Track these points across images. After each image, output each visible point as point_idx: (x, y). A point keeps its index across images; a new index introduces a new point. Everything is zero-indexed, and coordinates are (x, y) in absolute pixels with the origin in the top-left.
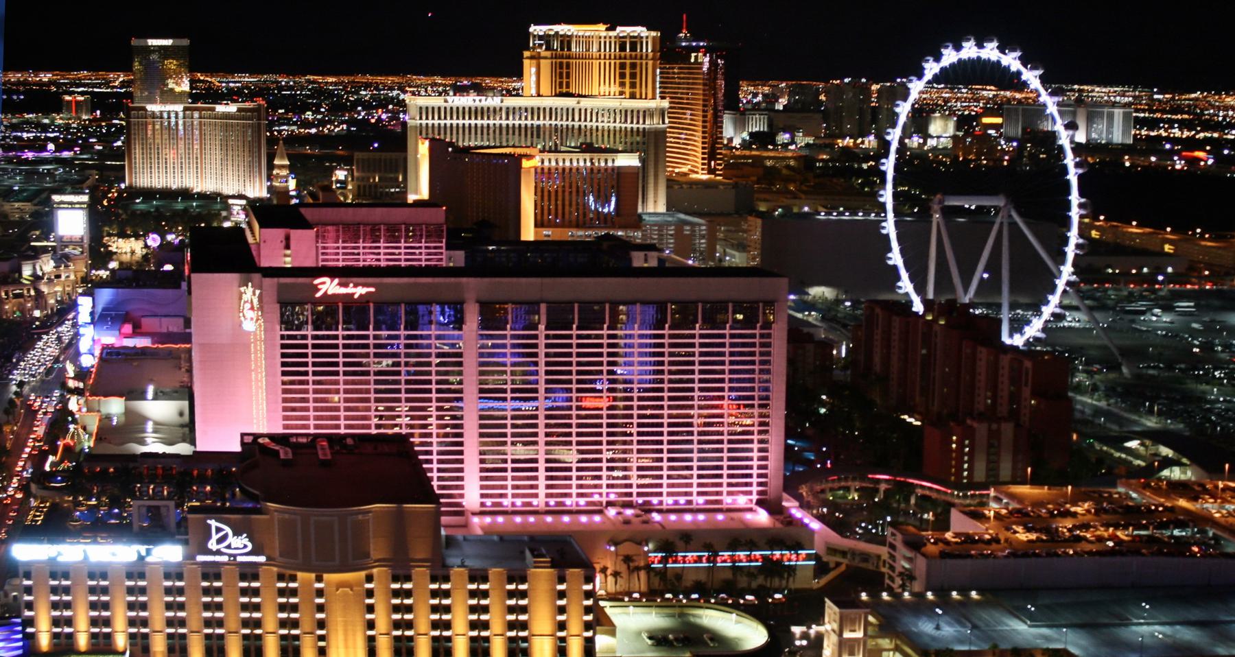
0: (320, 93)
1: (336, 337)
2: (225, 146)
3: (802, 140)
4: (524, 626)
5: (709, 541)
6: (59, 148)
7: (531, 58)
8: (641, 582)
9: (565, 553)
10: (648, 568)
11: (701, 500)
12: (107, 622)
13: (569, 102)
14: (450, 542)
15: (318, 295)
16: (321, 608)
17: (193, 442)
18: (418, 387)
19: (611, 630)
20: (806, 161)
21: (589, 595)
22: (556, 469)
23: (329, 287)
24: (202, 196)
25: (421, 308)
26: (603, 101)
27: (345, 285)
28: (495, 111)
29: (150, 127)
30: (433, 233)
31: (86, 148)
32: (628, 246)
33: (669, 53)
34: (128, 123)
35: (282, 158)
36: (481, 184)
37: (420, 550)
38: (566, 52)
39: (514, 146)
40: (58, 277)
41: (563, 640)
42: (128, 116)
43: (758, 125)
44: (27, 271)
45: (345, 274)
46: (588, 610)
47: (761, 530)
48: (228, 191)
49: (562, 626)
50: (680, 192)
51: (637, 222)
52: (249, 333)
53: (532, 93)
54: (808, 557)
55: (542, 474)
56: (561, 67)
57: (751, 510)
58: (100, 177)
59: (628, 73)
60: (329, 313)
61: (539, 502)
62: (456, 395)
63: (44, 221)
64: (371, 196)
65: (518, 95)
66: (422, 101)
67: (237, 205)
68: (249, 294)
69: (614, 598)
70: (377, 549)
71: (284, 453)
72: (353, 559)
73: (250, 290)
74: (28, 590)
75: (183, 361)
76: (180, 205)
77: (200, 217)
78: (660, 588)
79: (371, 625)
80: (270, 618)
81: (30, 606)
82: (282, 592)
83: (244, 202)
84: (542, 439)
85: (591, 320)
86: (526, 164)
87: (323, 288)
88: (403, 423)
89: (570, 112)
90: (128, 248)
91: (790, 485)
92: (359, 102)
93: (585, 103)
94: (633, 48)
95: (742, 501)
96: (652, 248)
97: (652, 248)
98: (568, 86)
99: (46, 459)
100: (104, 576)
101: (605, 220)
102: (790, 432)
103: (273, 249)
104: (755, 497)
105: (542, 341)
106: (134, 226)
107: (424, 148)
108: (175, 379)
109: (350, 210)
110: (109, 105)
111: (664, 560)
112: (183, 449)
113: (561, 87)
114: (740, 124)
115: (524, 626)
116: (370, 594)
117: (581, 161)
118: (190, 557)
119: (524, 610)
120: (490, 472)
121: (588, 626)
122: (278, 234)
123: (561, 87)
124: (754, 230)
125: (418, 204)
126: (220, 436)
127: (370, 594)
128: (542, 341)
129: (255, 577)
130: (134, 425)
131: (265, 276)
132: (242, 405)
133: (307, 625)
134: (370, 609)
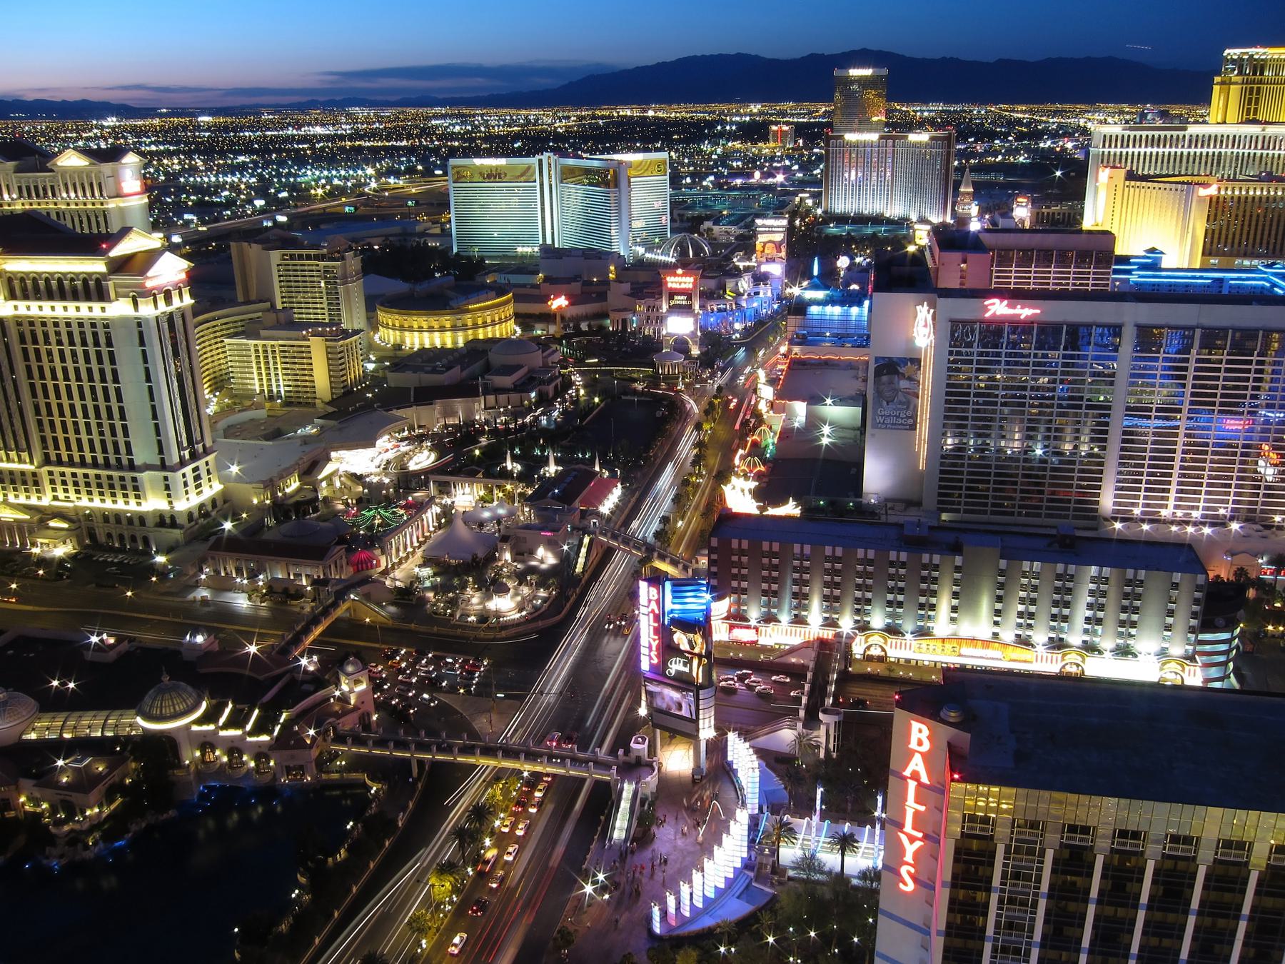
7: (1222, 83)
15: (987, 315)
25: (1082, 331)
29: (847, 155)
34: (827, 151)
35: (967, 186)
38: (1258, 77)
39: (1192, 175)
40: (757, 293)
42: (827, 145)
56: (1251, 93)
63: (746, 244)
64: (1044, 224)
65: (1204, 122)
68: (924, 313)
77: (887, 241)
83: (928, 227)
89: (1253, 140)
93: (1271, 130)
98: (1255, 113)
99: (736, 451)
103: (953, 269)
113: (1248, 114)
123: (1248, 114)
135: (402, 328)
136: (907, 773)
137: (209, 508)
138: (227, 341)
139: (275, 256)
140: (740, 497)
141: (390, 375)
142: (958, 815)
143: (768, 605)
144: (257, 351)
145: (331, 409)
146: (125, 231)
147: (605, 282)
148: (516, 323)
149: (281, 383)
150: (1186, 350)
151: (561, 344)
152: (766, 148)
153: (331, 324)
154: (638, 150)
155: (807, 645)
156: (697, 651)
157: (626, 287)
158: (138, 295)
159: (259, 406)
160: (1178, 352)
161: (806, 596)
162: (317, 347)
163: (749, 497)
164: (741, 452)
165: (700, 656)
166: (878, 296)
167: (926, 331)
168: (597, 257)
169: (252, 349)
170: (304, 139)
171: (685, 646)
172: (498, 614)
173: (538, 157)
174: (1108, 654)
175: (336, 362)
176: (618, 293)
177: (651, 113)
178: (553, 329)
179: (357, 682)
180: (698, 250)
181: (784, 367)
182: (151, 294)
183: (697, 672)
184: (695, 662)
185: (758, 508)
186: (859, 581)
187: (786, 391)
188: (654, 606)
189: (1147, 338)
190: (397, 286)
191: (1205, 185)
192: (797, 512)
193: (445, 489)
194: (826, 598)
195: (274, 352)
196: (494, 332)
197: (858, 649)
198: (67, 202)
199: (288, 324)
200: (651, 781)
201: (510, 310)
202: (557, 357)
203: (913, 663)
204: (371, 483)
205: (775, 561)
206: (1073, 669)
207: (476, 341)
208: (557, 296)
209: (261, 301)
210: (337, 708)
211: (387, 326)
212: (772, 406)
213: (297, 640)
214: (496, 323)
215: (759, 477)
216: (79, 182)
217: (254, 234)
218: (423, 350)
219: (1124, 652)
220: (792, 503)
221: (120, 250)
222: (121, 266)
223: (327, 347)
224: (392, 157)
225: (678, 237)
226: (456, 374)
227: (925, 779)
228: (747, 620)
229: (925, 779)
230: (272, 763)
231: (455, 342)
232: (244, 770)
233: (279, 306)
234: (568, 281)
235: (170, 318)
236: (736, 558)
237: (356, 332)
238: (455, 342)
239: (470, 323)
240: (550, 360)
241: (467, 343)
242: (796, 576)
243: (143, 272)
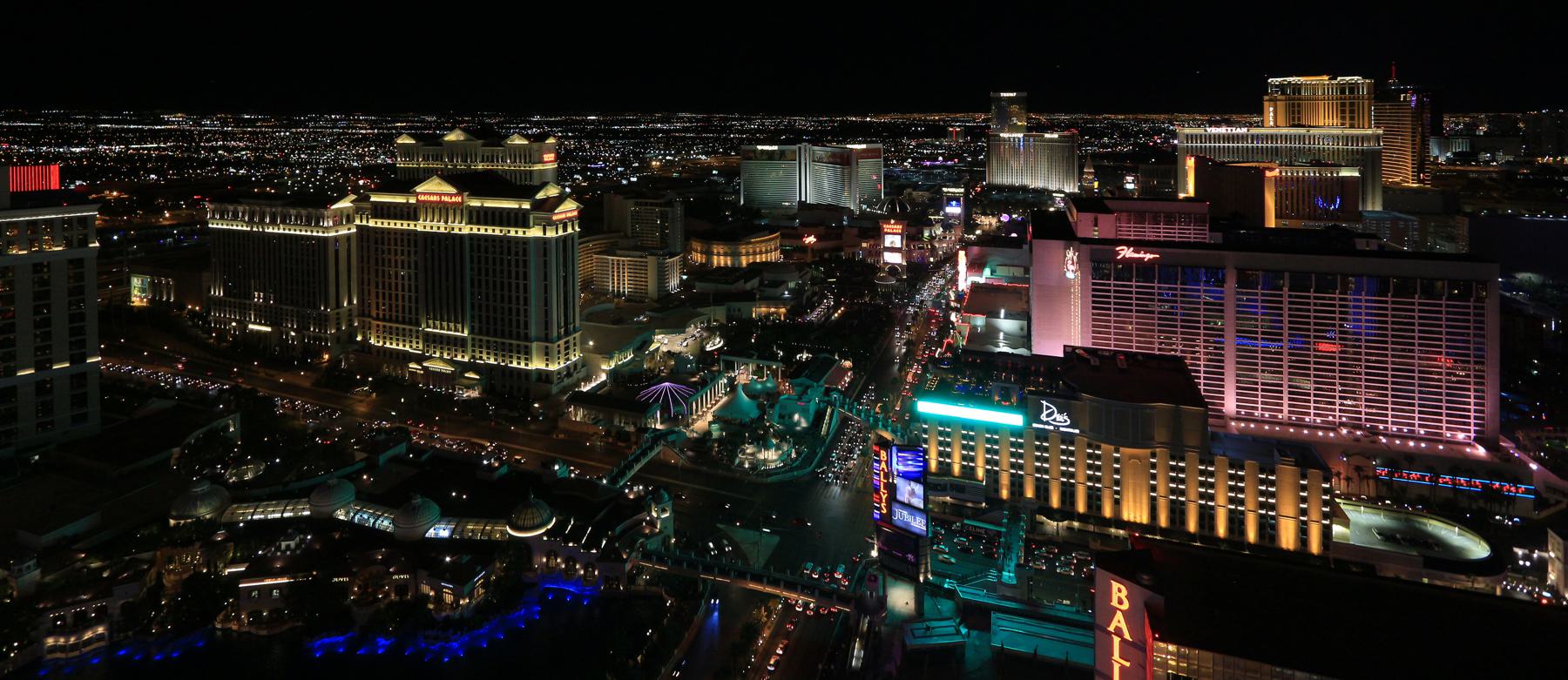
0: (1114, 126)
2: (1050, 160)
3: (1502, 158)
4: (1272, 507)
5: (1433, 464)
6: (945, 160)
8: (1370, 489)
9: (1308, 457)
10: (1376, 478)
11: (1422, 431)
12: (972, 459)
13: (1302, 131)
14: (1214, 436)
16: (1117, 471)
17: (1029, 348)
18: (1190, 325)
19: (1345, 522)
20: (1508, 174)
21: (1326, 491)
22: (1297, 395)
23: (1127, 252)
24: (1035, 191)
26: (1327, 127)
28: (1242, 138)
30: (1199, 220)
31: (962, 160)
32: (1350, 235)
33: (1381, 95)
36: (1231, 185)
37: (1192, 439)
41: (1304, 523)
43: (1460, 146)
44: (926, 234)
45: (1138, 245)
46: (1326, 503)
47: (1477, 461)
48: (1053, 186)
49: (1304, 512)
50: (1394, 196)
51: (1359, 217)
53: (1272, 123)
54: (1527, 491)
55: (1286, 396)
57: (1469, 445)
58: (972, 174)
59: (1348, 107)
61: (1284, 415)
62: (1220, 333)
64: (1147, 193)
66: (1188, 131)
69: (1347, 497)
70: (1161, 434)
71: (1094, 362)
72: (1141, 439)
74: (925, 431)
76: (1020, 196)
78: (1383, 495)
79: (1153, 488)
80: (1082, 474)
81: (926, 441)
82: (1090, 456)
84: (1285, 370)
85: (1326, 285)
86: (1268, 174)
88: (1178, 348)
89: (1301, 138)
90: (988, 222)
91: (1507, 429)
92: (1141, 131)
93: (1313, 131)
94: (1352, 90)
95: (1461, 436)
96: (1374, 236)
97: (1374, 236)
100: (996, 432)
101: (1331, 216)
102: (1503, 387)
104: (1472, 435)
105: (1286, 299)
106: (993, 208)
107: (1191, 163)
108: (1022, 305)
111: (1390, 474)
112: (1022, 351)
114: (1444, 147)
115: (1272, 507)
116: (1154, 466)
117: (1312, 173)
118: (1028, 423)
119: (1273, 495)
120: (1242, 391)
121: (1325, 516)
122: (1089, 216)
124: (1463, 227)
125: (1188, 199)
126: (1050, 346)
127: (1154, 466)
128: (1286, 299)
129: (1072, 443)
130: (991, 333)
132: (1065, 331)
133: (1107, 481)
134: (1154, 477)
139: (631, 202)
146: (544, 185)
147: (840, 226)
157: (855, 231)
158: (547, 224)
159: (611, 301)
168: (835, 210)
180: (903, 208)
182: (554, 224)
191: (1271, 169)
193: (730, 366)
198: (507, 166)
207: (755, 263)
214: (764, 251)
216: (517, 153)
217: (619, 189)
218: (719, 268)
221: (540, 196)
222: (540, 206)
234: (815, 225)
235: (565, 239)
241: (749, 265)
243: (552, 210)
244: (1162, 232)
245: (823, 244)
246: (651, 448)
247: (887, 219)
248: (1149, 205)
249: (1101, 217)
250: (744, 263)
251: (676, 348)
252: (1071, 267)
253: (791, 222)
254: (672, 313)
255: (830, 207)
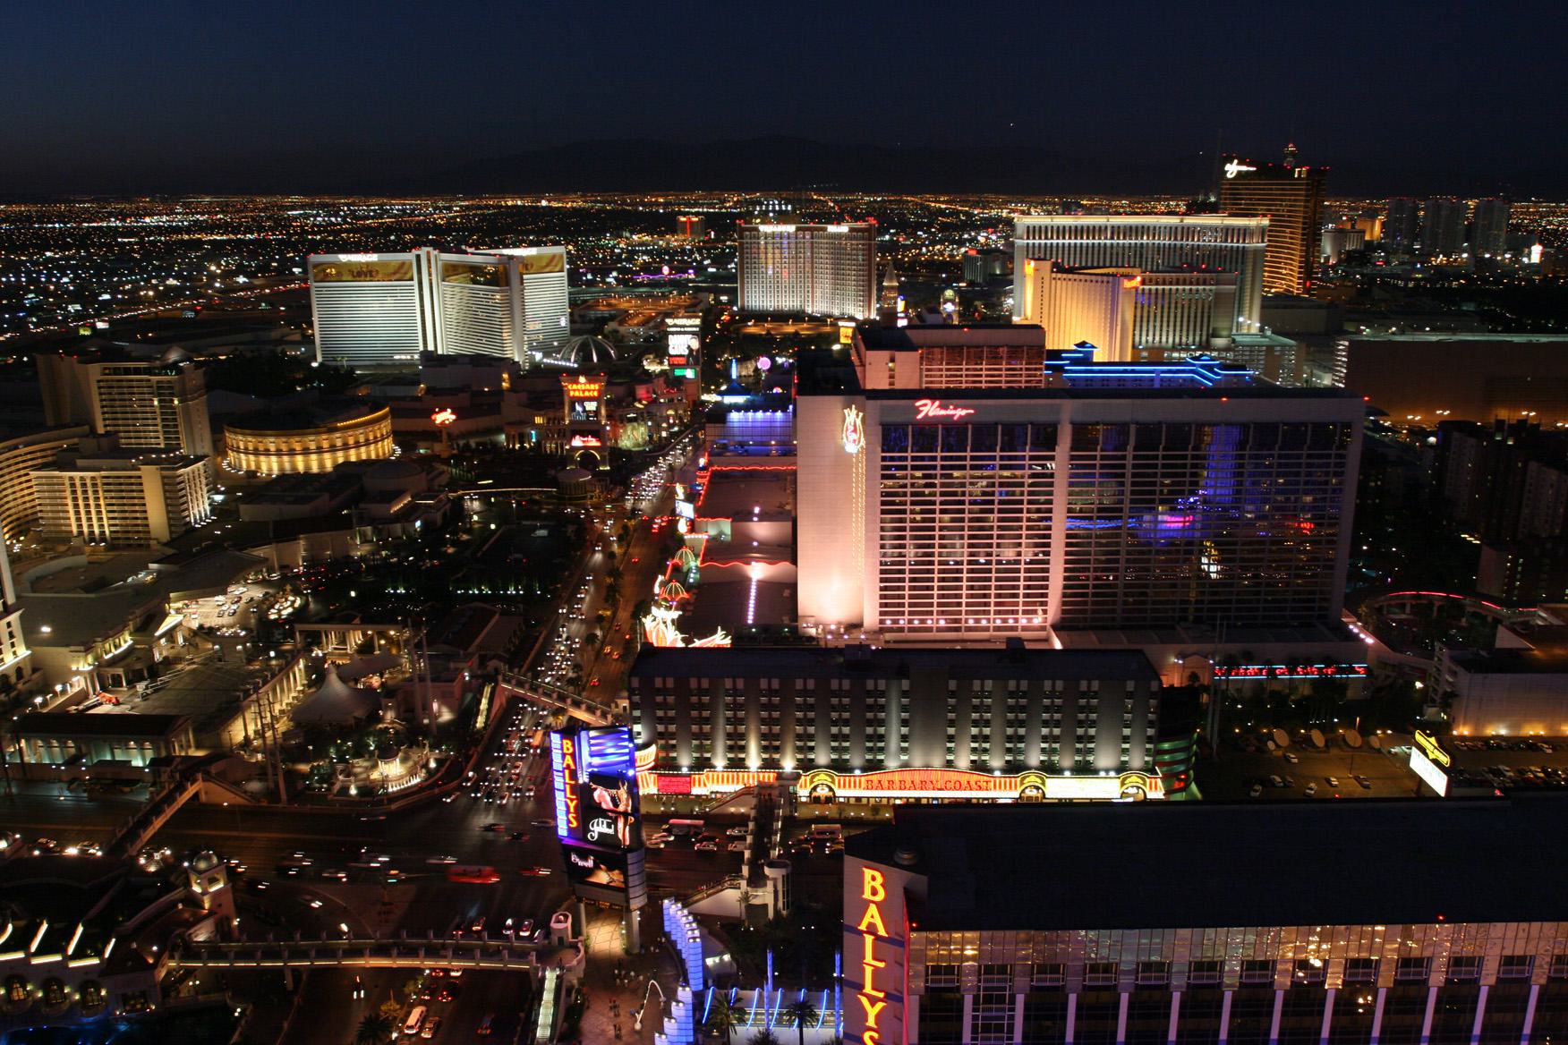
1: (934, 459)
23: (929, 409)
27: (946, 408)
52: (851, 455)
60: (926, 434)
67: (846, 329)
68: (852, 416)
73: (854, 411)
75: (788, 482)
87: (925, 409)
109: (955, 332)
110: (722, 224)
131: (869, 398)
135: (256, 452)
136: (863, 927)
137: (13, 679)
138: (34, 474)
139: (95, 371)
140: (661, 627)
141: (242, 507)
142: (921, 968)
143: (700, 748)
144: (73, 485)
145: (170, 551)
148: (395, 442)
149: (105, 522)
150: (1123, 447)
151: (449, 464)
152: (674, 241)
153: (166, 451)
154: (532, 244)
155: (747, 791)
156: (621, 808)
157: (523, 396)
159: (77, 551)
160: (1115, 450)
161: (742, 736)
162: (150, 478)
163: (672, 628)
164: (660, 578)
165: (625, 814)
166: (801, 400)
167: (854, 436)
168: (488, 365)
169: (67, 482)
170: (129, 232)
171: (607, 804)
172: (385, 781)
173: (415, 252)
174: (1067, 774)
175: (174, 498)
176: (510, 409)
177: (544, 203)
178: (438, 448)
179: (213, 881)
181: (705, 481)
183: (623, 832)
184: (620, 825)
185: (683, 640)
186: (799, 714)
187: (707, 510)
188: (569, 760)
189: (1083, 437)
190: (253, 401)
192: (727, 642)
193: (315, 639)
194: (763, 736)
195: (94, 485)
196: (368, 453)
197: (803, 793)
199: (112, 451)
200: (575, 961)
201: (386, 427)
202: (444, 479)
203: (864, 801)
204: (223, 636)
205: (706, 699)
206: (1034, 793)
207: (347, 463)
208: (443, 410)
209: (77, 425)
210: (187, 915)
211: (238, 451)
212: (693, 527)
213: (133, 834)
215: (681, 606)
218: (283, 477)
219: (1085, 769)
220: (720, 633)
223: (163, 477)
224: (240, 253)
225: (578, 340)
226: (324, 502)
227: (882, 932)
228: (678, 768)
229: (882, 932)
230: (103, 993)
231: (322, 465)
232: (65, 1007)
233: (101, 430)
236: (672, 695)
237: (198, 459)
238: (322, 465)
239: (339, 443)
240: (436, 483)
241: (337, 467)
242: (729, 714)
244: (984, 374)
245: (469, 424)
246: (181, 788)
247: (573, 374)
248: (982, 336)
249: (899, 355)
250: (329, 466)
251: (213, 621)
252: (849, 432)
253: (398, 388)
254: (198, 560)
255: (479, 361)
